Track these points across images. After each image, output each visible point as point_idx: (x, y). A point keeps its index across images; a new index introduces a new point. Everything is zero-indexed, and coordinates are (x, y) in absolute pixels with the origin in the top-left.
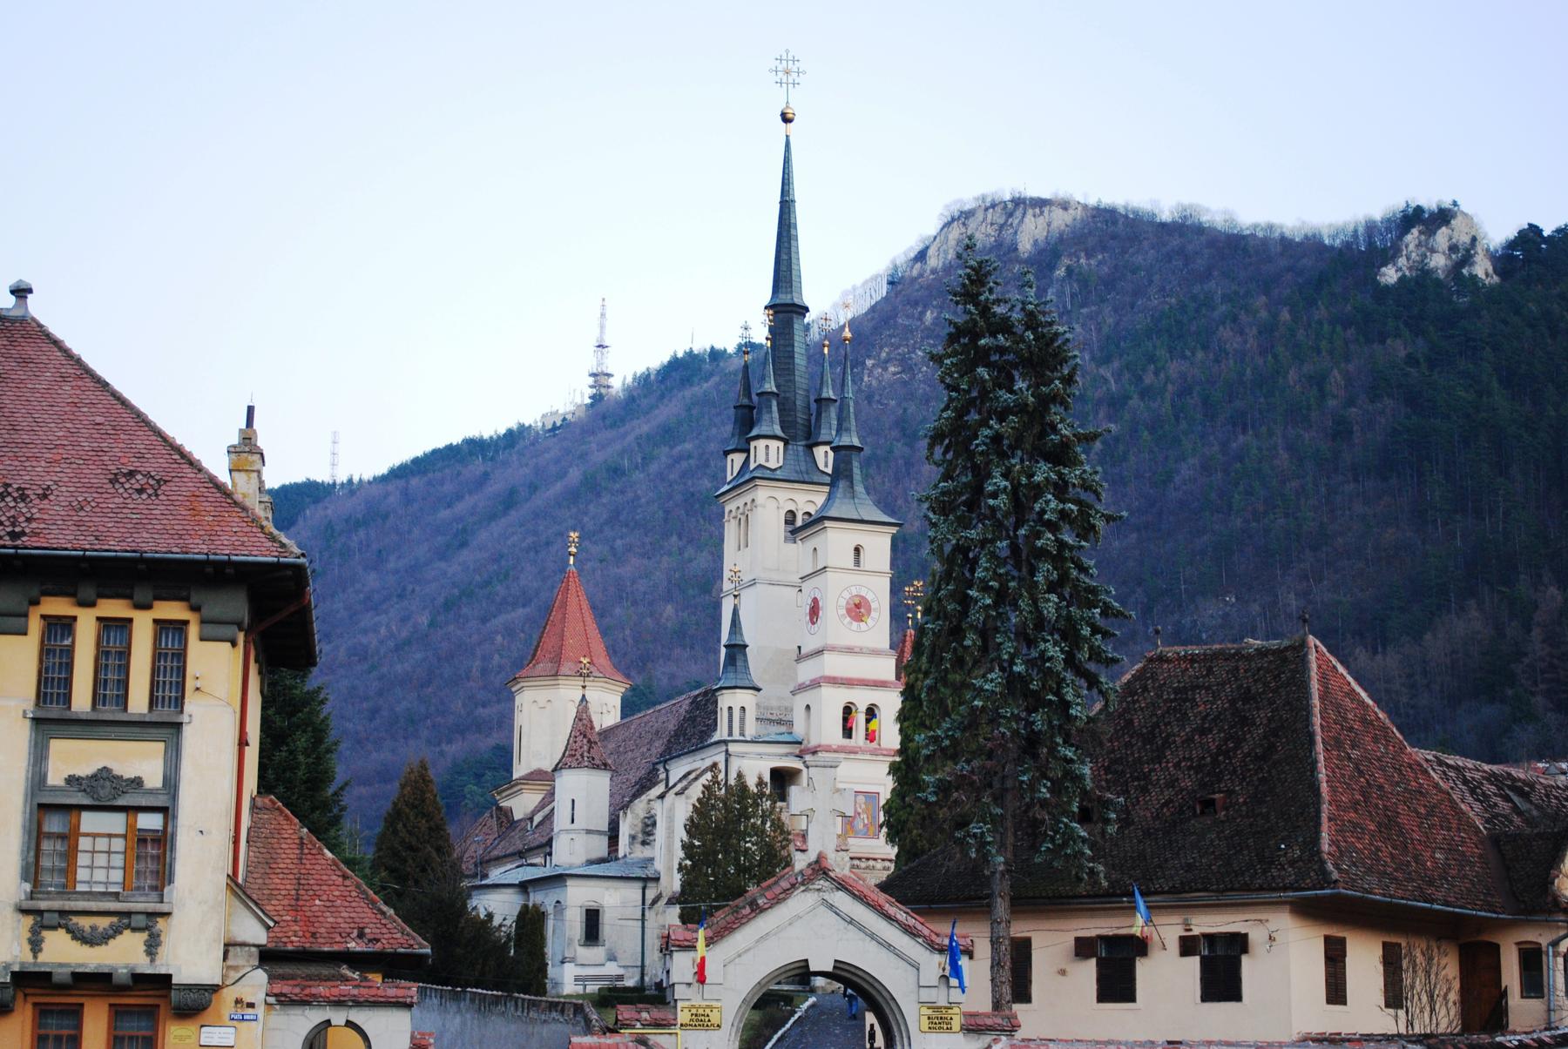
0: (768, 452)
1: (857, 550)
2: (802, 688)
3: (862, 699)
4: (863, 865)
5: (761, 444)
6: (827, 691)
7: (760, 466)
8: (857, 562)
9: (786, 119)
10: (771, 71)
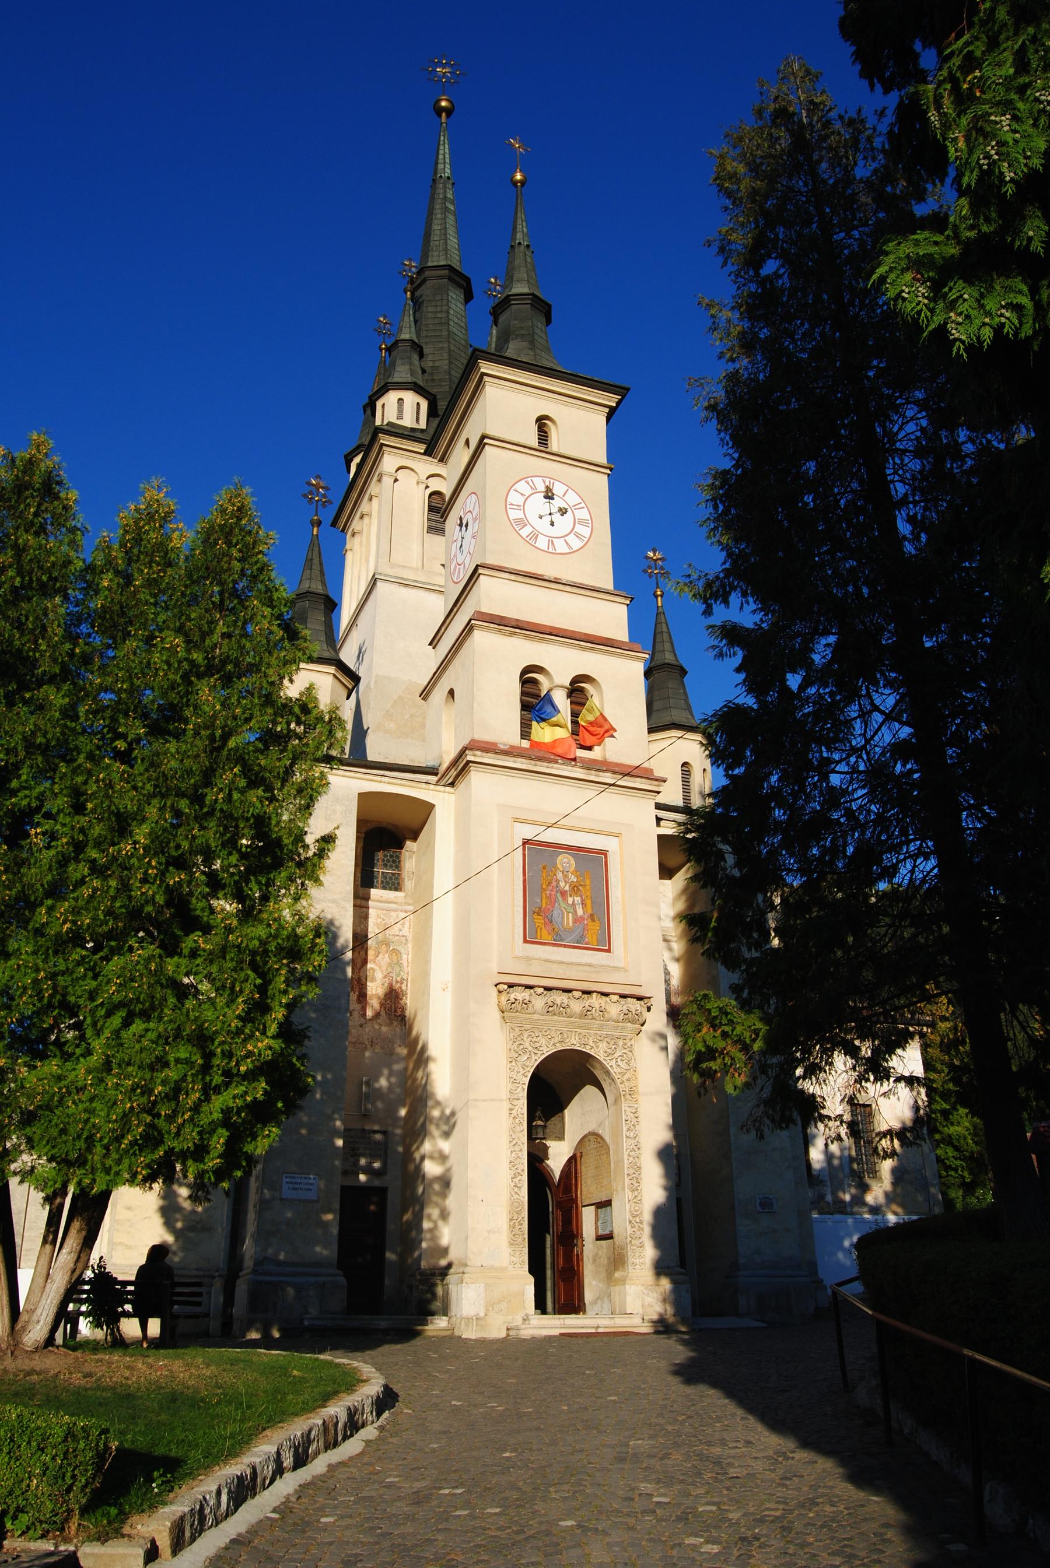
0: (402, 408)
1: (542, 423)
3: (561, 664)
4: (576, 1006)
5: (391, 398)
6: (483, 639)
7: (389, 424)
8: (543, 436)
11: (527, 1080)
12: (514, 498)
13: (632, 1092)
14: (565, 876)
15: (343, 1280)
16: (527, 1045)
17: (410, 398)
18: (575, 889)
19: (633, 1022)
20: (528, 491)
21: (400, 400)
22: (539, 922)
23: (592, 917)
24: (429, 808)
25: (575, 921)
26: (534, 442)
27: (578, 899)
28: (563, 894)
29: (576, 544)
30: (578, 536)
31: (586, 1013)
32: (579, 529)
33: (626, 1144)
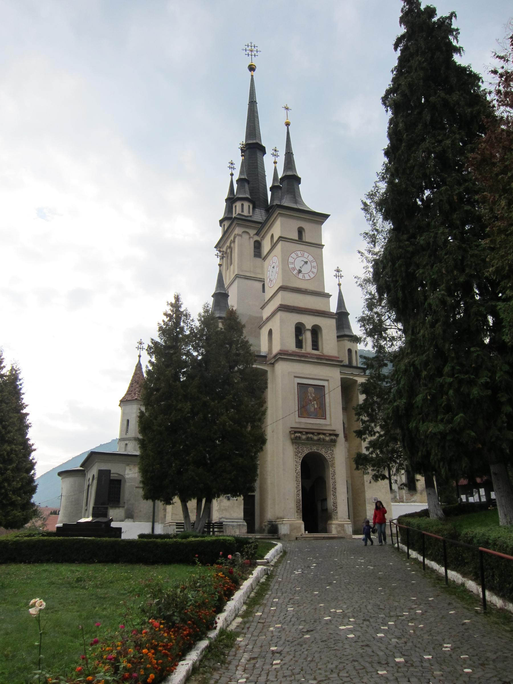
2: (269, 319)
3: (309, 322)
4: (316, 438)
5: (238, 204)
7: (239, 214)
9: (252, 68)
10: (243, 50)
11: (300, 461)
12: (291, 260)
13: (333, 464)
14: (311, 395)
15: (245, 523)
16: (300, 450)
17: (246, 204)
18: (314, 399)
19: (333, 442)
20: (295, 257)
21: (242, 205)
22: (303, 410)
23: (320, 408)
24: (266, 372)
25: (315, 409)
26: (297, 238)
27: (315, 402)
28: (310, 400)
29: (312, 276)
30: (313, 272)
31: (319, 440)
32: (313, 270)
33: (331, 481)
